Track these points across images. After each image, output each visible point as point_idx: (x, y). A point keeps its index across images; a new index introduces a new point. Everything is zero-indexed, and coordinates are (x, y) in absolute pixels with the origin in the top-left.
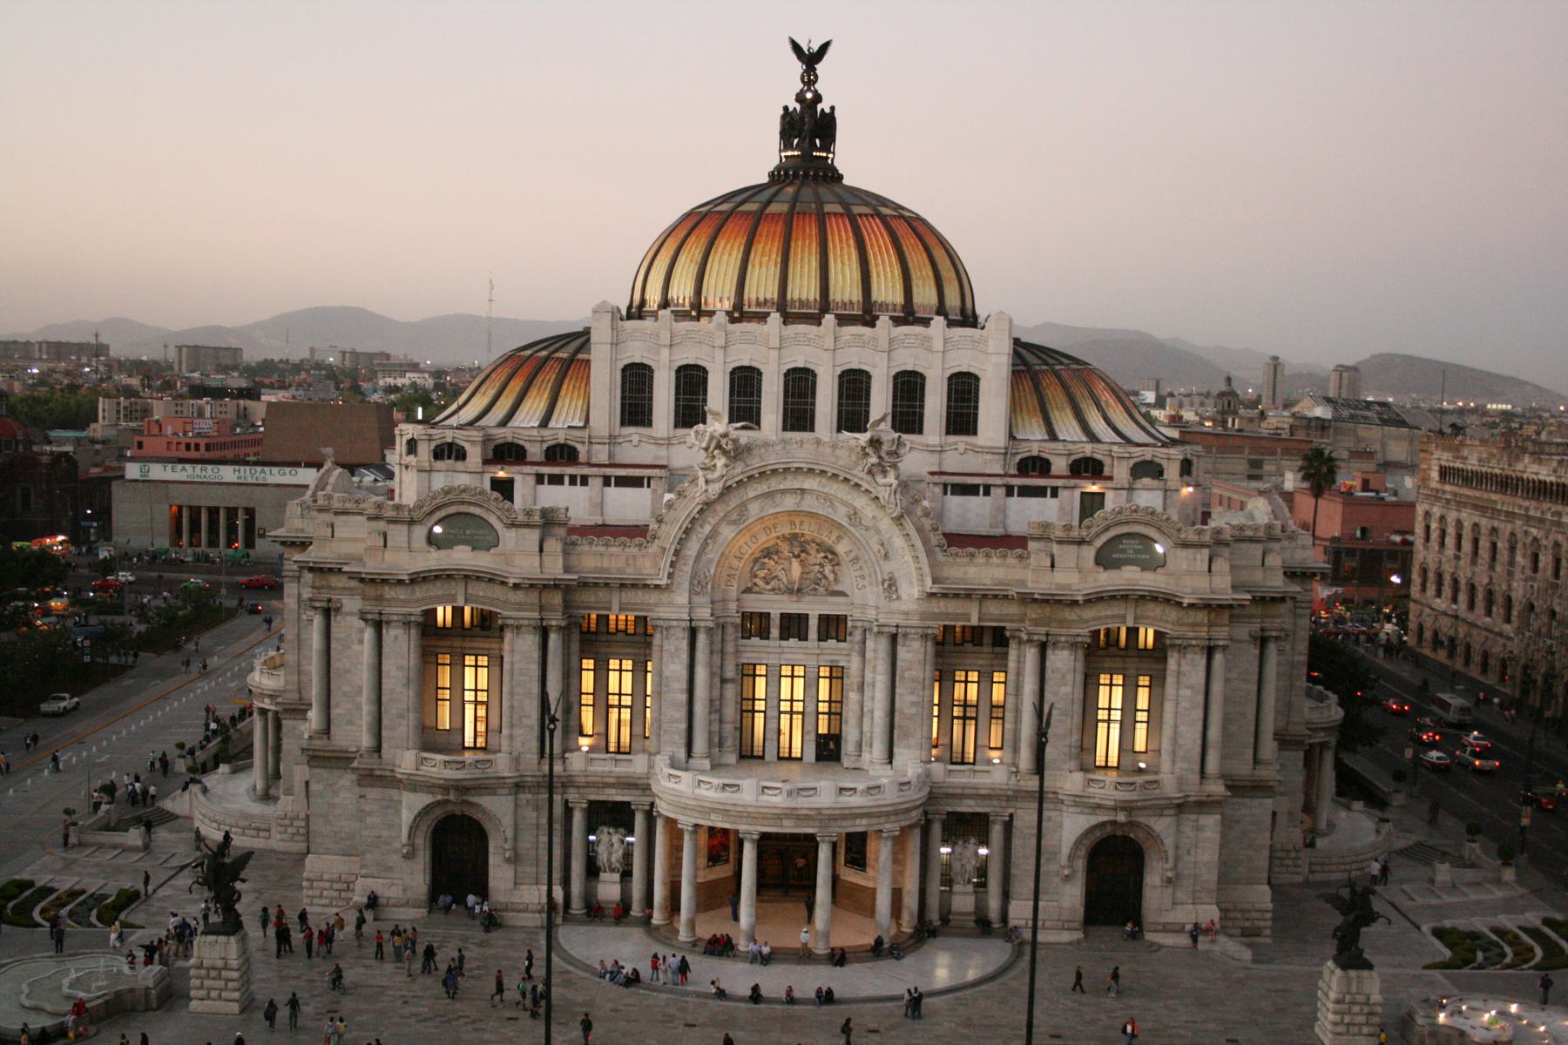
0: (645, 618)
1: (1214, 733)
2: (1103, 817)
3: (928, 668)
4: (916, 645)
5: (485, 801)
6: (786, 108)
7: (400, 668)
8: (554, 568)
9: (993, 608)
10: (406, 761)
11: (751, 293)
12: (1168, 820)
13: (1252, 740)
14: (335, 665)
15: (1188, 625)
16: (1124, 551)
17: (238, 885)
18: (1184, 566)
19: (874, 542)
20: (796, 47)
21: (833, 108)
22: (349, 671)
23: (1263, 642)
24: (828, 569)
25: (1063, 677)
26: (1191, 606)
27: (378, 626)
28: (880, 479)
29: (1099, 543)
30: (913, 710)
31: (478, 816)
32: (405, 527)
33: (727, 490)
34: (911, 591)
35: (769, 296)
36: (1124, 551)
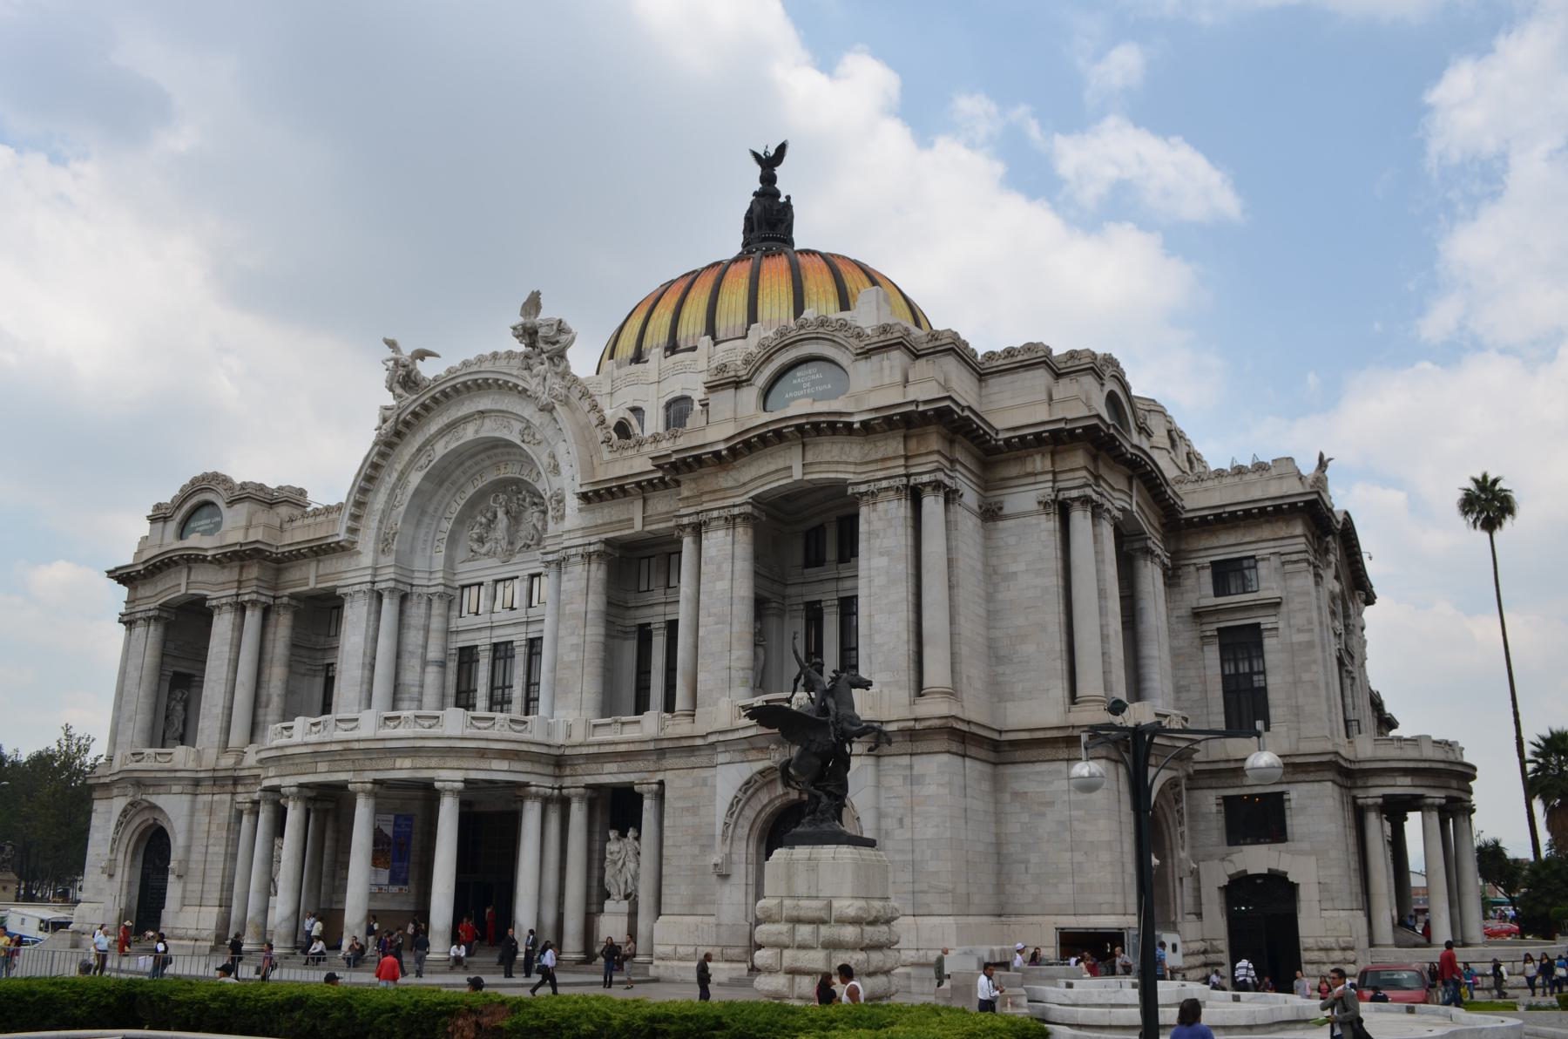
1: (935, 620)
5: (160, 800)
8: (257, 535)
9: (661, 504)
11: (647, 344)
13: (1061, 666)
15: (876, 461)
16: (799, 387)
18: (869, 385)
19: (545, 459)
23: (1063, 510)
25: (719, 568)
29: (762, 379)
30: (573, 656)
31: (165, 825)
34: (572, 503)
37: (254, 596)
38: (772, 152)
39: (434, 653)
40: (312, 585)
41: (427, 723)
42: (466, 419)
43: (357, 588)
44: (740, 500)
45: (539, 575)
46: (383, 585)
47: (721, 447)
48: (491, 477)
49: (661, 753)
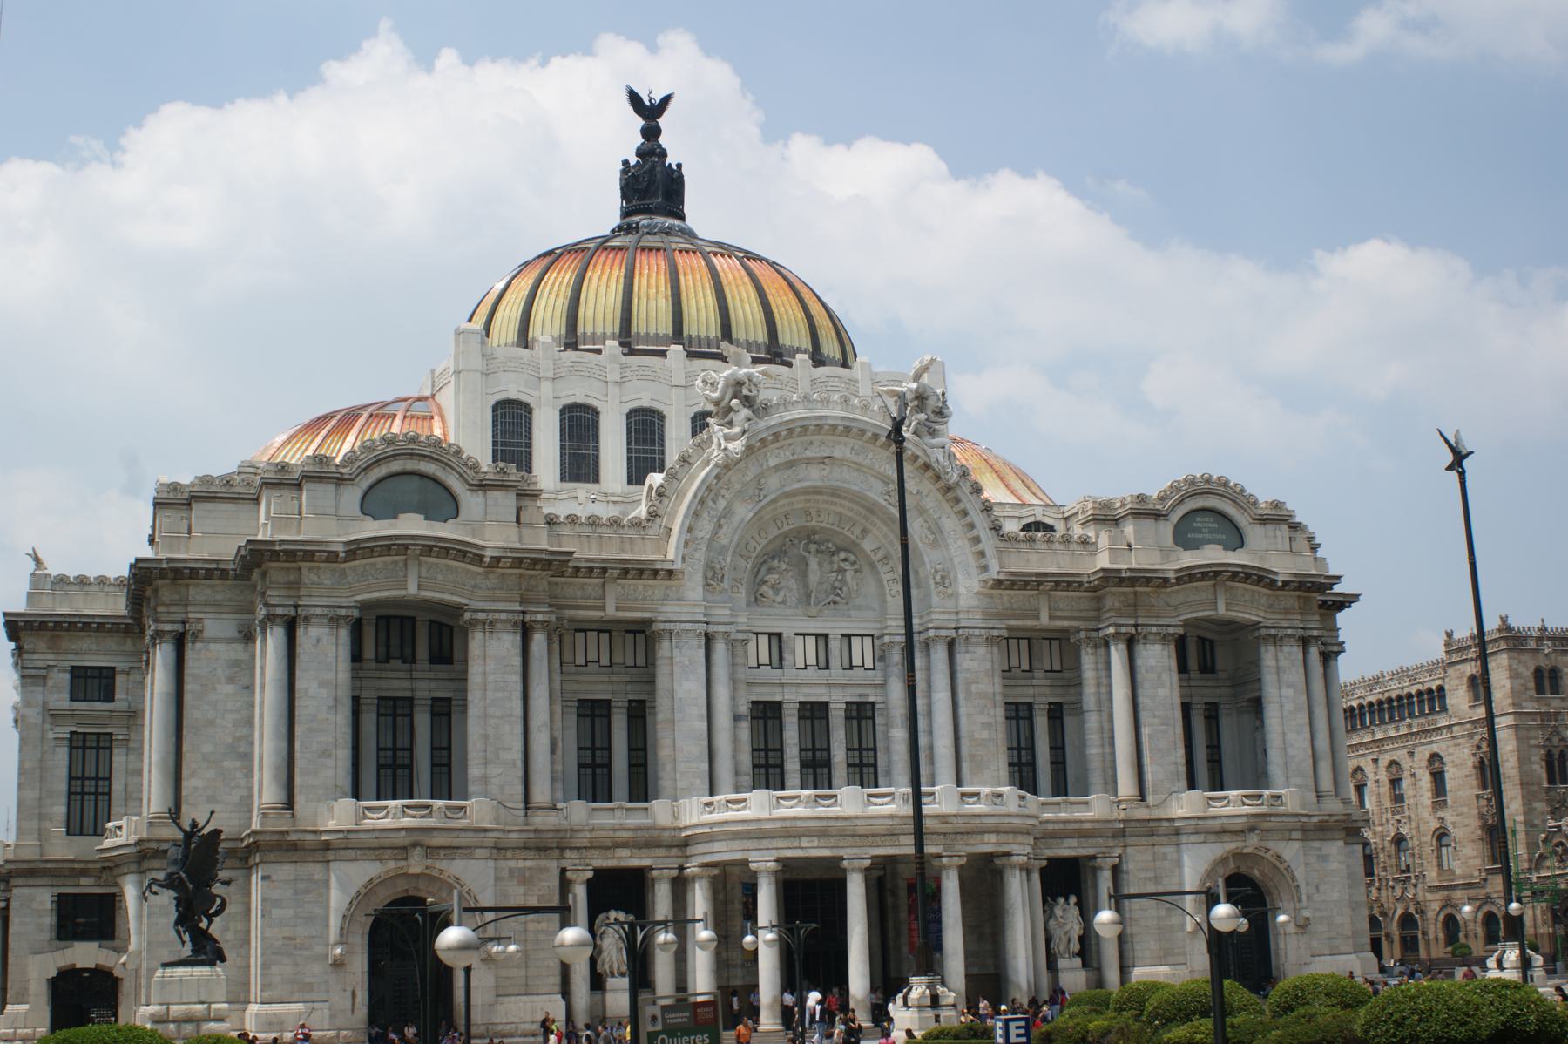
0: (650, 622)
2: (1231, 845)
3: (998, 679)
4: (981, 651)
5: (455, 867)
6: (626, 163)
7: (322, 684)
10: (337, 815)
11: (639, 326)
12: (1296, 845)
14: (190, 714)
16: (1198, 530)
17: (217, 889)
20: (634, 99)
21: (679, 166)
22: (212, 723)
24: (849, 575)
25: (1159, 677)
26: (1286, 583)
27: (291, 627)
28: (928, 439)
32: (331, 487)
33: (749, 449)
34: (968, 587)
35: (661, 331)
36: (1198, 530)
37: (553, 618)
38: (658, 99)
39: (744, 709)
40: (611, 612)
41: (998, 801)
42: (809, 461)
43: (688, 626)
44: (1174, 622)
45: (849, 636)
46: (721, 628)
47: (1171, 575)
48: (796, 523)
49: (1122, 834)
